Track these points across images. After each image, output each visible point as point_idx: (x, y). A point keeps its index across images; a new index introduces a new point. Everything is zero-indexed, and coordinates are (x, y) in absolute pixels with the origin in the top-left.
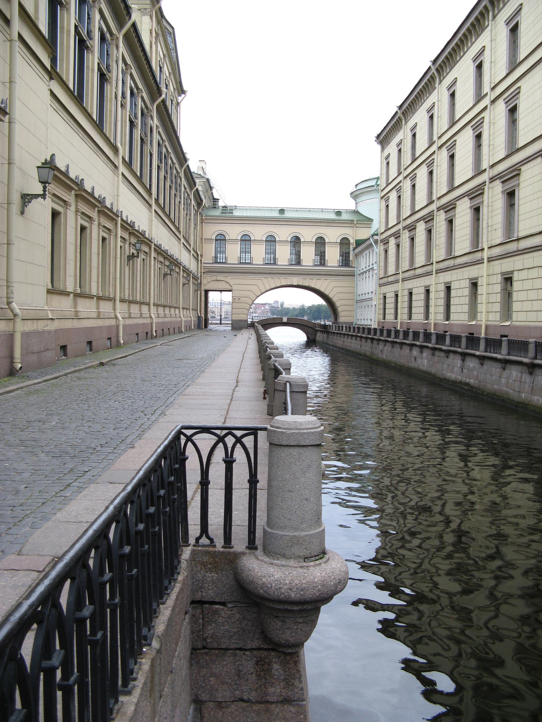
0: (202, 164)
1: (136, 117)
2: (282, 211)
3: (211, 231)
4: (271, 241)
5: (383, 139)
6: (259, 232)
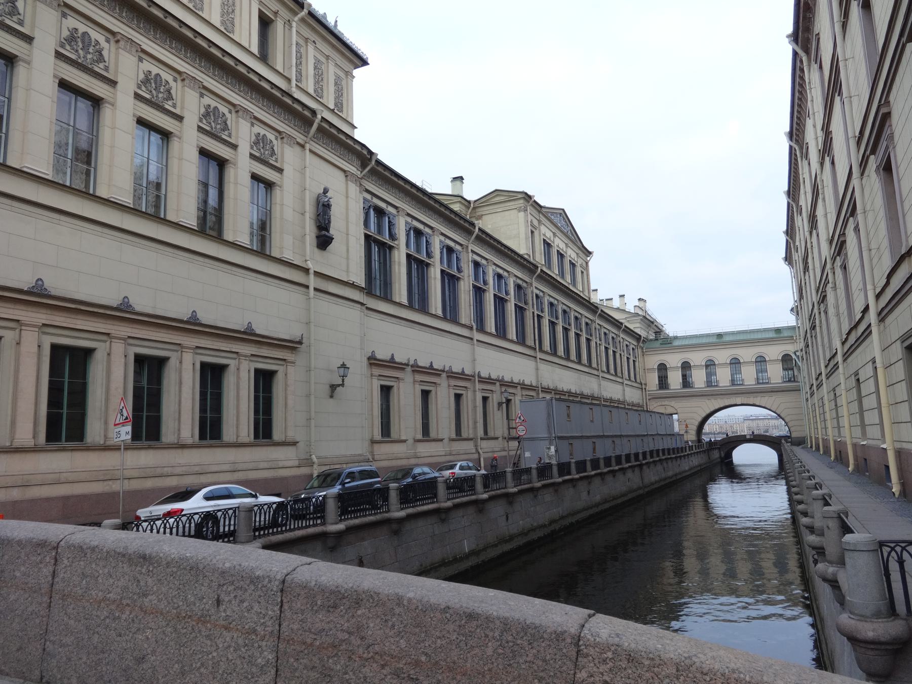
0: (641, 304)
1: (507, 293)
2: (720, 336)
3: (653, 361)
4: (710, 365)
5: (788, 259)
6: (697, 358)
